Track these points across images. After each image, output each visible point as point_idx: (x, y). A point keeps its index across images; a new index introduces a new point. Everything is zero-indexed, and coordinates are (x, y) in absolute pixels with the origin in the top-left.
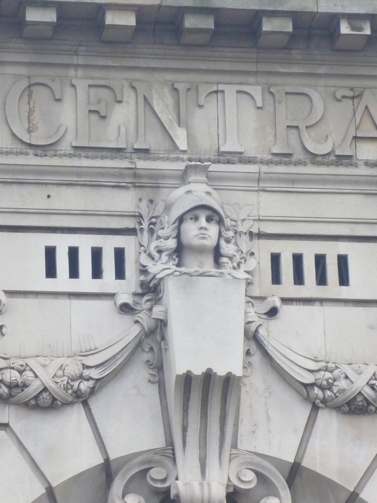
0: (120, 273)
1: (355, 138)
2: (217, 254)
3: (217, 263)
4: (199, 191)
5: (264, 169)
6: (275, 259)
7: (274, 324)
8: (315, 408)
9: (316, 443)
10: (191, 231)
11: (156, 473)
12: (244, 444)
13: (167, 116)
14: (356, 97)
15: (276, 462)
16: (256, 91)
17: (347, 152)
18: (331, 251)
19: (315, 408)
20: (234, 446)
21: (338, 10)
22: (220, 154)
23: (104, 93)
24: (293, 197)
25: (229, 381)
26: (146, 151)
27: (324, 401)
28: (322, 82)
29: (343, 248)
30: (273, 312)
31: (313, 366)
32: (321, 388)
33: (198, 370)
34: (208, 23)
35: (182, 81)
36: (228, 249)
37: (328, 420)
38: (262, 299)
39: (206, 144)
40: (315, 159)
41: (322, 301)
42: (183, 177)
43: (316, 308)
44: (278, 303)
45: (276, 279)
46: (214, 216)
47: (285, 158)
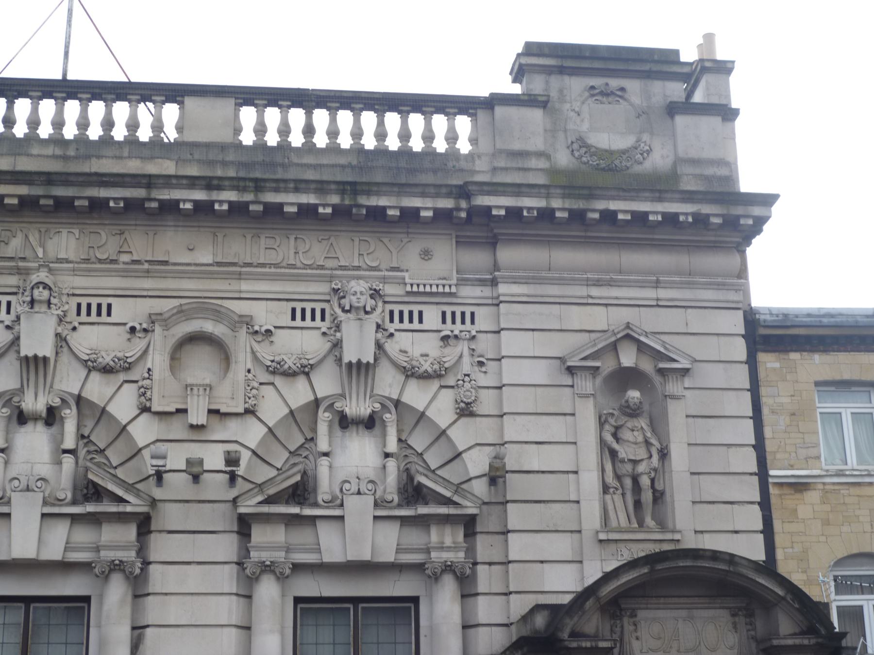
0: (8, 312)
1: (120, 252)
2: (49, 303)
3: (49, 308)
4: (42, 276)
5: (76, 265)
6: (79, 305)
7: (75, 334)
8: (90, 371)
9: (89, 386)
10: (36, 292)
11: (16, 399)
12: (56, 386)
13: (34, 243)
14: (122, 233)
15: (71, 394)
16: (76, 232)
17: (115, 258)
18: (105, 302)
19: (90, 371)
20: (51, 387)
21: (108, 196)
22: (58, 259)
23: (8, 233)
24: (89, 278)
25: (45, 359)
26: (24, 258)
27: (93, 367)
28: (108, 227)
29: (110, 300)
30: (74, 329)
31: (89, 352)
32: (92, 362)
33: (30, 354)
34: (51, 202)
35: (43, 228)
36: (53, 300)
37: (95, 377)
38: (71, 323)
39: (52, 255)
40: (100, 261)
41: (99, 324)
42: (38, 270)
43: (95, 327)
44: (76, 325)
45: (79, 314)
46: (46, 286)
47: (87, 261)
